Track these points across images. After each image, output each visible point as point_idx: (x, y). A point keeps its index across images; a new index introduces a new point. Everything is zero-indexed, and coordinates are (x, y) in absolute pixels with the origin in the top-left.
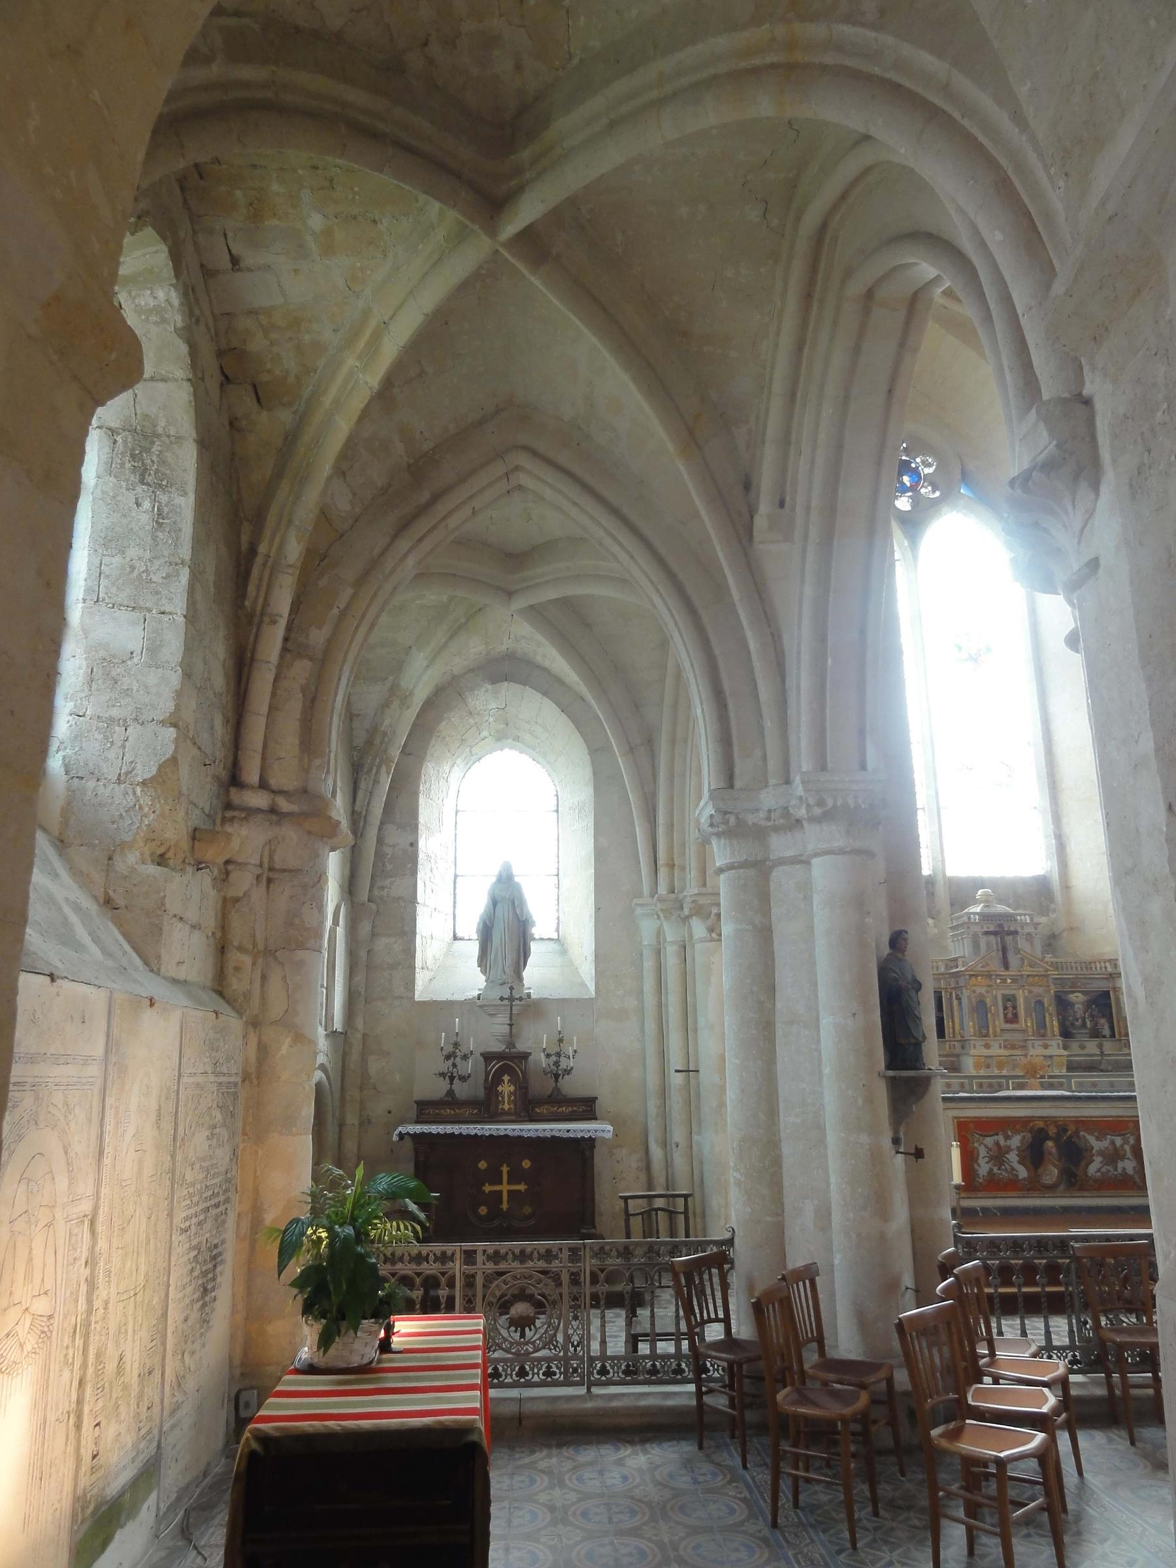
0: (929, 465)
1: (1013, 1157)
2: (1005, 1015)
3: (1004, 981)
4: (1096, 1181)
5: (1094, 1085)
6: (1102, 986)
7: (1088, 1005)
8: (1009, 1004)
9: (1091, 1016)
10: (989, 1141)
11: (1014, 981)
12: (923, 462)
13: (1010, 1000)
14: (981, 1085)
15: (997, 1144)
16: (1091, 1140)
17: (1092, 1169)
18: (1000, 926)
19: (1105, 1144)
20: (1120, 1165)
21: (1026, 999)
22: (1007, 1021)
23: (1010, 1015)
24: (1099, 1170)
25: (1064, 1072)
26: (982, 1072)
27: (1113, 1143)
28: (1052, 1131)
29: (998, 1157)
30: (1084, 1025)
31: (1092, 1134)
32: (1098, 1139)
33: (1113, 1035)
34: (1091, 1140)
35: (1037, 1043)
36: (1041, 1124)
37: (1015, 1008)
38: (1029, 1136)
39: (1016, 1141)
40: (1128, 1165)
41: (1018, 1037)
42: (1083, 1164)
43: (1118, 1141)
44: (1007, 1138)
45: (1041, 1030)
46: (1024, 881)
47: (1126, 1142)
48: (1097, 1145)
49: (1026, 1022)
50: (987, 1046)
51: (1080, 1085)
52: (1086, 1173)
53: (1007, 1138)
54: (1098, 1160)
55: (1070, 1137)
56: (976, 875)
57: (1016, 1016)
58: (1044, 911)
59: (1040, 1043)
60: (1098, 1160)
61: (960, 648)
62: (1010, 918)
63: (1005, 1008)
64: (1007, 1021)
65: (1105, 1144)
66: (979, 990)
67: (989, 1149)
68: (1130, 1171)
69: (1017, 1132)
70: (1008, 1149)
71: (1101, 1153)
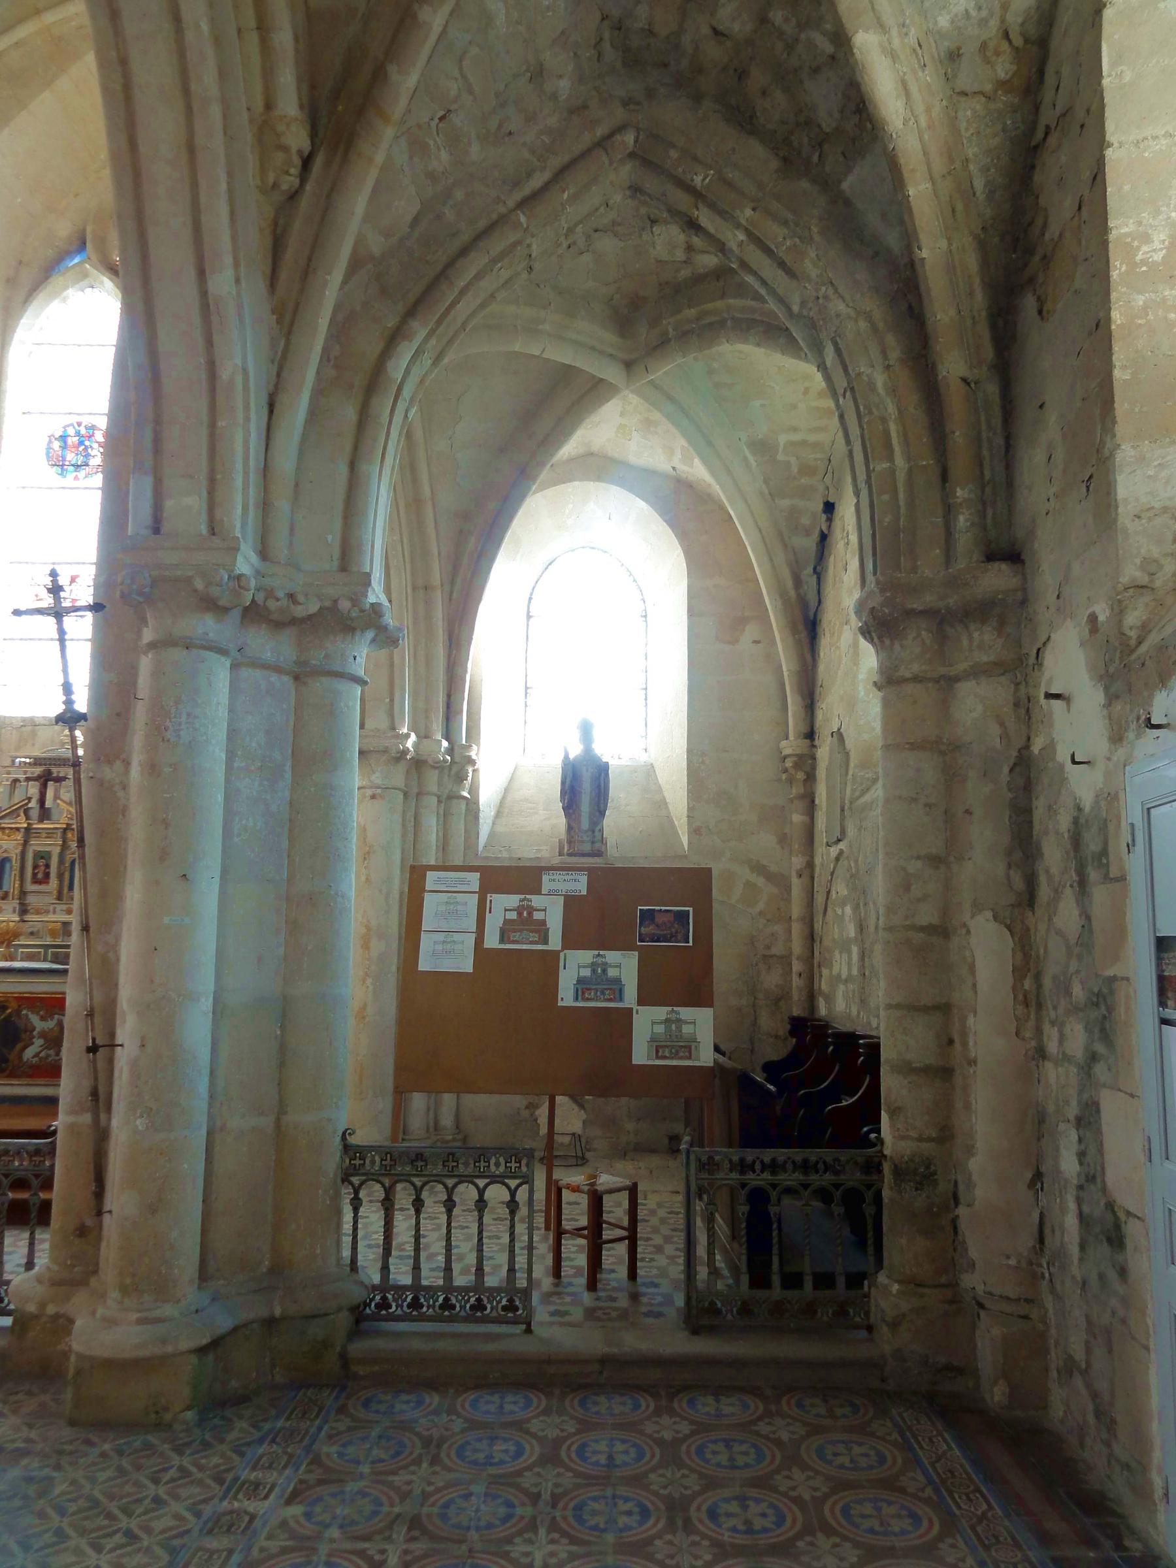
2: (34, 875)
4: (32, 1067)
8: (41, 862)
16: (35, 1019)
17: (29, 1053)
18: (49, 772)
21: (61, 856)
22: (36, 881)
23: (40, 876)
24: (37, 1055)
31: (38, 1013)
32: (43, 1019)
34: (35, 1019)
35: (59, 908)
37: (47, 866)
42: (19, 1046)
49: (54, 883)
52: (20, 1057)
54: (38, 1042)
55: (10, 1015)
57: (47, 875)
59: (65, 907)
60: (38, 1042)
63: (35, 867)
71: (43, 1035)
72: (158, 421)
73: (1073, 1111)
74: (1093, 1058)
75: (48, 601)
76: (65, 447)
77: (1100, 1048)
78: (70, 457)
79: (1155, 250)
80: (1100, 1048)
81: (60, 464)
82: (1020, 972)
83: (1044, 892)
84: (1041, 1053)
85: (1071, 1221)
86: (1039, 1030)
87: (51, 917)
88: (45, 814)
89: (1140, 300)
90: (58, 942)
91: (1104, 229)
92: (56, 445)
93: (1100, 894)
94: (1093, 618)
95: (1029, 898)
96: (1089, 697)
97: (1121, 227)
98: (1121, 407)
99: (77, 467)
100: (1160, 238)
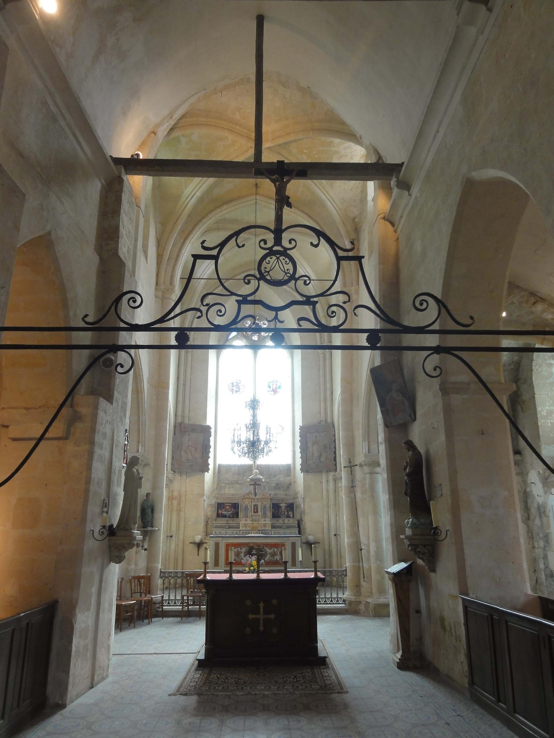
0: (265, 324)
1: (242, 555)
3: (254, 500)
5: (279, 533)
6: (291, 501)
7: (286, 507)
9: (287, 511)
10: (235, 550)
11: (257, 500)
12: (263, 323)
13: (256, 506)
14: (243, 533)
15: (238, 551)
18: (255, 483)
19: (272, 551)
20: (275, 557)
22: (254, 512)
25: (270, 528)
26: (244, 529)
27: (274, 550)
28: (256, 547)
29: (238, 554)
30: (284, 513)
33: (293, 517)
36: (252, 545)
37: (257, 508)
38: (248, 548)
39: (244, 550)
40: (278, 557)
41: (257, 518)
43: (276, 550)
44: (241, 549)
45: (265, 515)
46: (282, 466)
47: (278, 550)
48: (269, 551)
49: (260, 513)
50: (246, 520)
51: (275, 532)
53: (241, 549)
54: (269, 556)
56: (268, 464)
58: (289, 475)
60: (269, 556)
61: (270, 387)
62: (260, 480)
63: (254, 508)
64: (254, 512)
65: (272, 551)
66: (264, 503)
67: (235, 552)
68: (278, 559)
69: (244, 547)
70: (241, 552)
71: (270, 554)
72: (368, 432)
73: (542, 557)
74: (545, 546)
75: (349, 465)
76: (233, 386)
77: (547, 545)
78: (235, 388)
79: (544, 413)
80: (547, 545)
81: (232, 391)
82: (528, 532)
83: (532, 517)
84: (534, 547)
85: (543, 576)
86: (533, 543)
87: (260, 522)
88: (256, 495)
89: (543, 421)
90: (263, 529)
91: (536, 409)
92: (231, 385)
93: (545, 519)
94: (539, 472)
95: (528, 518)
96: (539, 485)
97: (539, 409)
98: (541, 439)
99: (236, 392)
100: (545, 411)
